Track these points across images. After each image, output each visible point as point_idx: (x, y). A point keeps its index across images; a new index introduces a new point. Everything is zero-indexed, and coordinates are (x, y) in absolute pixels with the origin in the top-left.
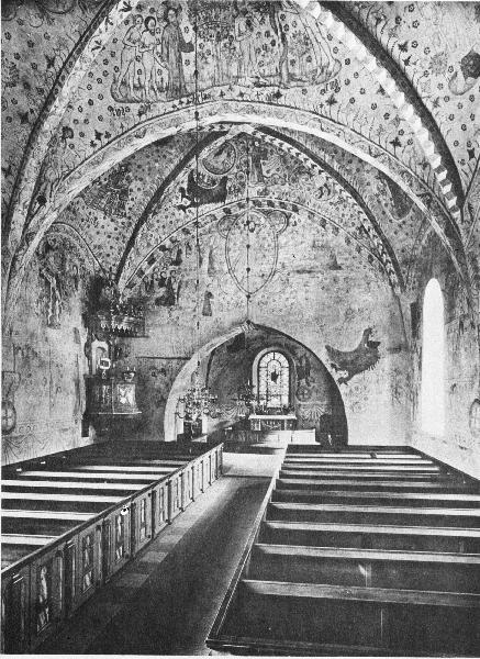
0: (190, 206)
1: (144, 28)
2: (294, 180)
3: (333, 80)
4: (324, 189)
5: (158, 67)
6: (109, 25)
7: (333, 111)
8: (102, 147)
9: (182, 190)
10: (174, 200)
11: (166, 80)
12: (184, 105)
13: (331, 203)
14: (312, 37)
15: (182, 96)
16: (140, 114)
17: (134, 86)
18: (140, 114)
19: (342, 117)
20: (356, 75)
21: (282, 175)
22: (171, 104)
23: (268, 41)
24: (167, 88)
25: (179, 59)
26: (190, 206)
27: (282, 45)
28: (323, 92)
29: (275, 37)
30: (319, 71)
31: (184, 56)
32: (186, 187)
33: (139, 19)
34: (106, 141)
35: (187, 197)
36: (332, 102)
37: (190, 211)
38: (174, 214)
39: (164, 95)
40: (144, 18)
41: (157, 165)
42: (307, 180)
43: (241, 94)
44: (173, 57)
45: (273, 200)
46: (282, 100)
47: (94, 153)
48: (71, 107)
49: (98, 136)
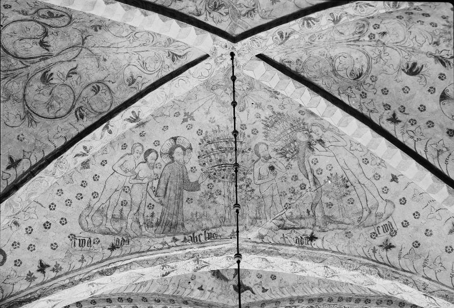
1: (142, 158)
3: (386, 222)
5: (149, 200)
6: (106, 132)
7: (392, 256)
8: (43, 283)
11: (157, 216)
12: (178, 243)
14: (352, 179)
15: (179, 233)
16: (113, 248)
17: (113, 216)
18: (113, 248)
19: (405, 263)
20: (416, 215)
22: (161, 240)
23: (296, 186)
24: (158, 224)
25: (180, 196)
27: (314, 188)
28: (374, 235)
29: (305, 181)
30: (366, 213)
31: (186, 194)
33: (140, 148)
34: (53, 274)
36: (389, 247)
39: (151, 230)
40: (146, 149)
43: (262, 237)
44: (171, 194)
46: (318, 243)
47: (29, 288)
48: (16, 223)
49: (42, 267)
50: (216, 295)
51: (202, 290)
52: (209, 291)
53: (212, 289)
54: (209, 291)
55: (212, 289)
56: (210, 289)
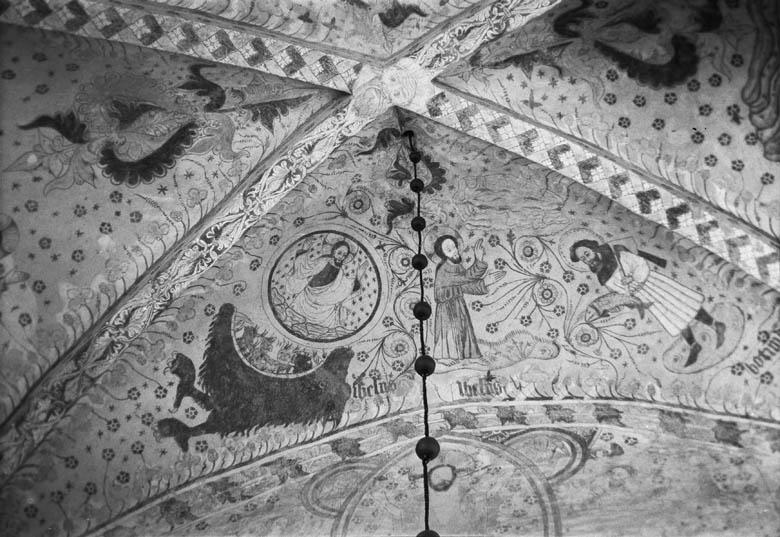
0: (206, 428)
2: (585, 338)
4: (700, 329)
9: (182, 366)
10: (148, 397)
13: (738, 369)
21: (543, 333)
26: (206, 428)
32: (197, 354)
35: (201, 399)
37: (202, 447)
38: (138, 449)
41: (105, 241)
42: (630, 324)
45: (519, 404)
50: (343, 34)
51: (310, 21)
52: (325, 24)
53: (333, 20)
54: (325, 24)
55: (333, 20)
56: (328, 20)
